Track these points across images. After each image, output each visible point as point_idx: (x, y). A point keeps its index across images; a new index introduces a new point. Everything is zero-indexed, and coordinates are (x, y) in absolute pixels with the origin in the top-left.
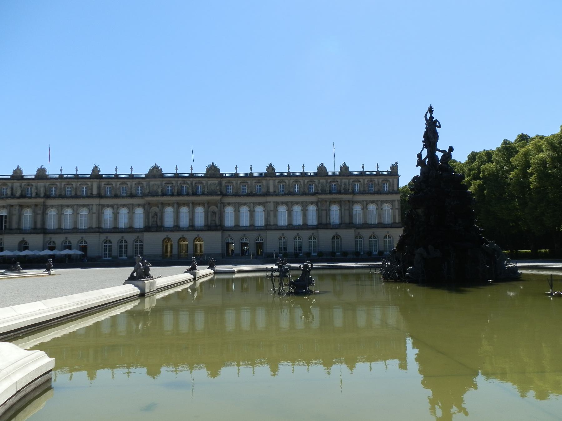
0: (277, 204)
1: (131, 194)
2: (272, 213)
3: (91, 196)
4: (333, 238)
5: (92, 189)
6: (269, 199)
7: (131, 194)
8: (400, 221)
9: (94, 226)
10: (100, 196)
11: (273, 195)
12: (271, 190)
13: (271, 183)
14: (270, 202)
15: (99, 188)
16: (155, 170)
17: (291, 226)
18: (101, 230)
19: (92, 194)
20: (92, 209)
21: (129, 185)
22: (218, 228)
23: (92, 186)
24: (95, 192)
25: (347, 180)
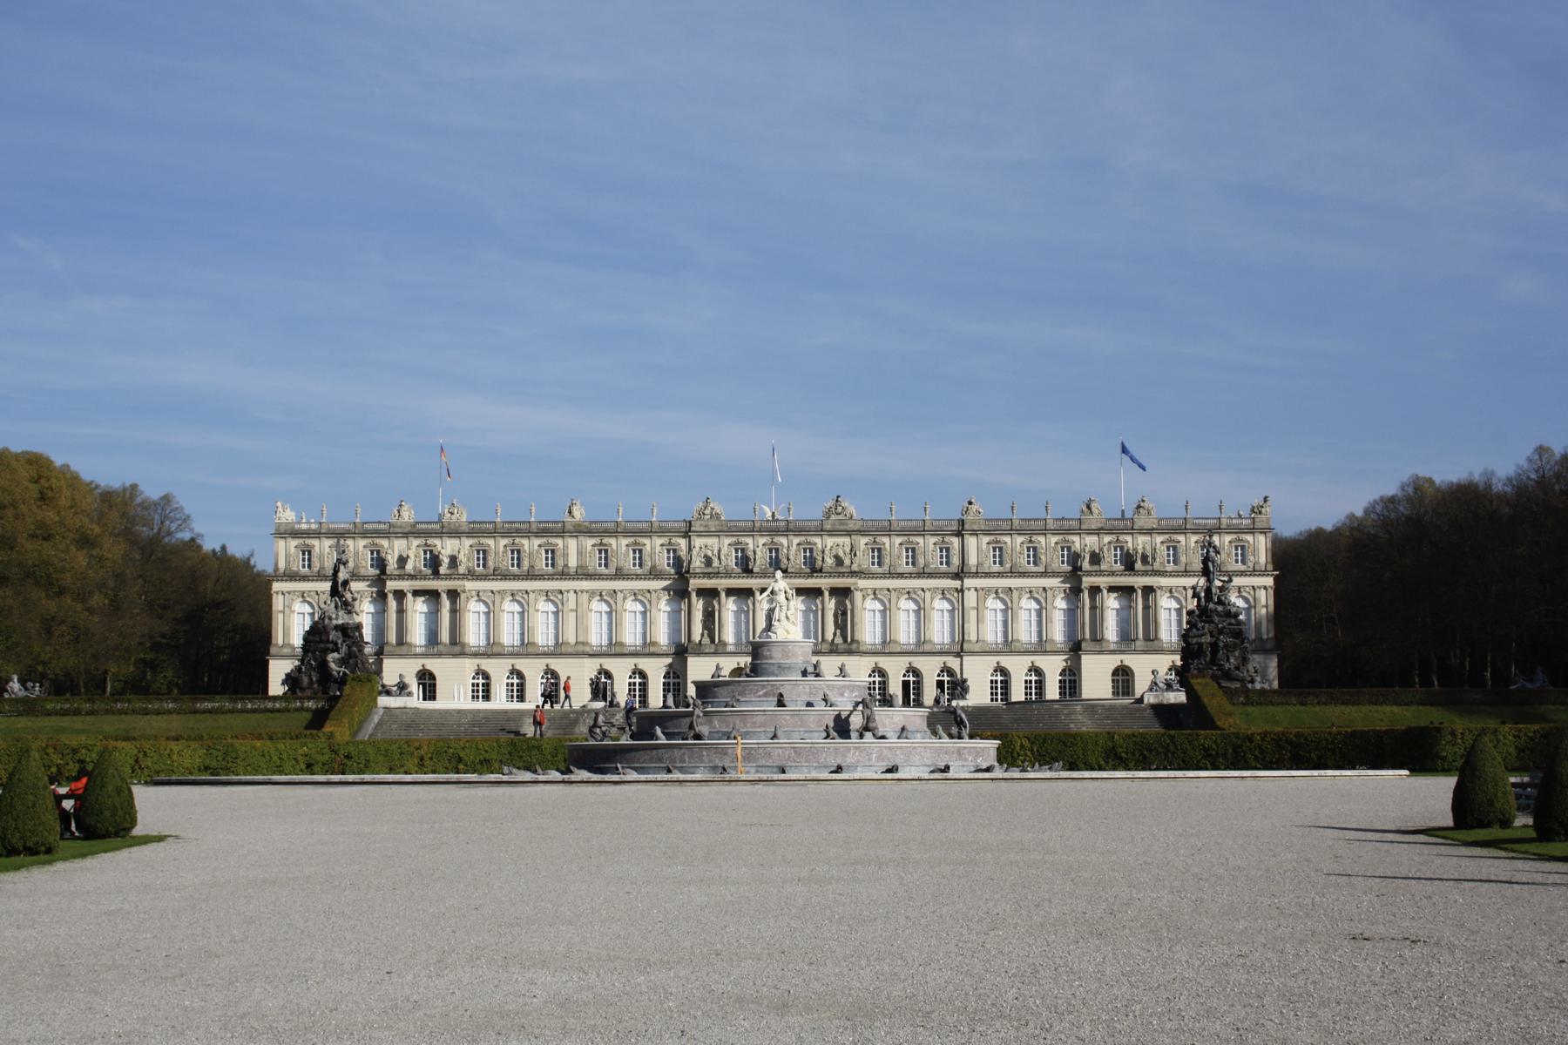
0: (983, 593)
1: (653, 568)
2: (973, 614)
3: (564, 575)
4: (1116, 672)
5: (565, 556)
6: (968, 582)
7: (653, 568)
8: (1272, 635)
9: (572, 640)
10: (584, 574)
11: (977, 575)
12: (972, 560)
13: (971, 541)
15: (580, 553)
18: (587, 649)
19: (566, 566)
22: (854, 646)
23: (566, 547)
24: (573, 563)
25: (1147, 538)
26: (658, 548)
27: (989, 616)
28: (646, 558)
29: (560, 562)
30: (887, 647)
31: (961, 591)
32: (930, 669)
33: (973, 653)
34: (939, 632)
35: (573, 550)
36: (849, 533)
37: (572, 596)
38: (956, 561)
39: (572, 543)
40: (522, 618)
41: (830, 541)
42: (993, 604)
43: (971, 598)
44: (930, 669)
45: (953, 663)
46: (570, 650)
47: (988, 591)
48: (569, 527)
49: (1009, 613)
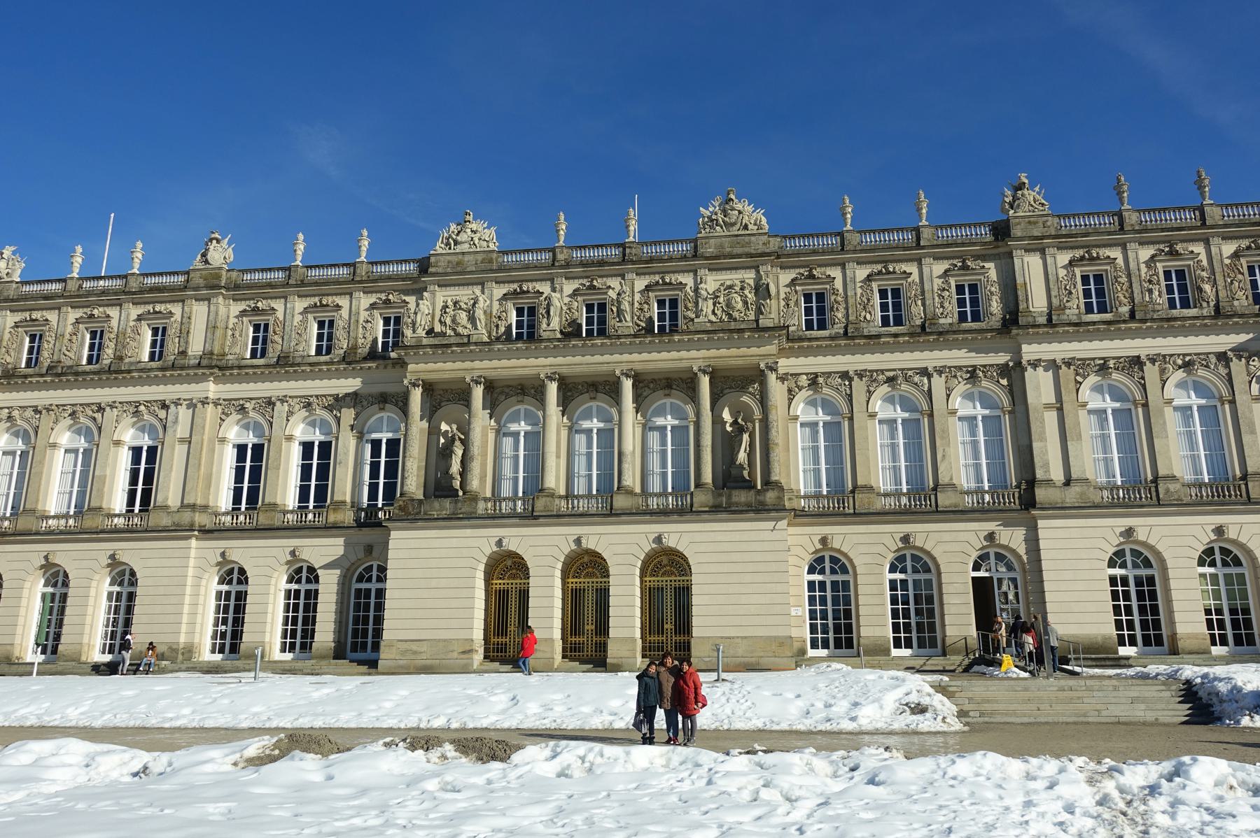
5: (184, 333)
10: (214, 365)
11: (1053, 325)
12: (1038, 302)
14: (1035, 364)
16: (463, 237)
17: (1173, 487)
18: (201, 519)
19: (183, 353)
20: (176, 421)
21: (345, 313)
22: (770, 496)
23: (187, 319)
24: (196, 346)
26: (364, 315)
27: (1087, 426)
28: (340, 333)
29: (172, 347)
30: (845, 501)
31: (1013, 374)
32: (955, 549)
33: (1061, 510)
34: (964, 463)
35: (202, 324)
36: (754, 260)
37: (184, 413)
38: (996, 306)
39: (199, 311)
40: (86, 464)
41: (712, 282)
42: (1092, 396)
43: (1040, 386)
44: (955, 549)
45: (1014, 538)
46: (165, 521)
47: (1081, 366)
48: (197, 279)
49: (1136, 420)
